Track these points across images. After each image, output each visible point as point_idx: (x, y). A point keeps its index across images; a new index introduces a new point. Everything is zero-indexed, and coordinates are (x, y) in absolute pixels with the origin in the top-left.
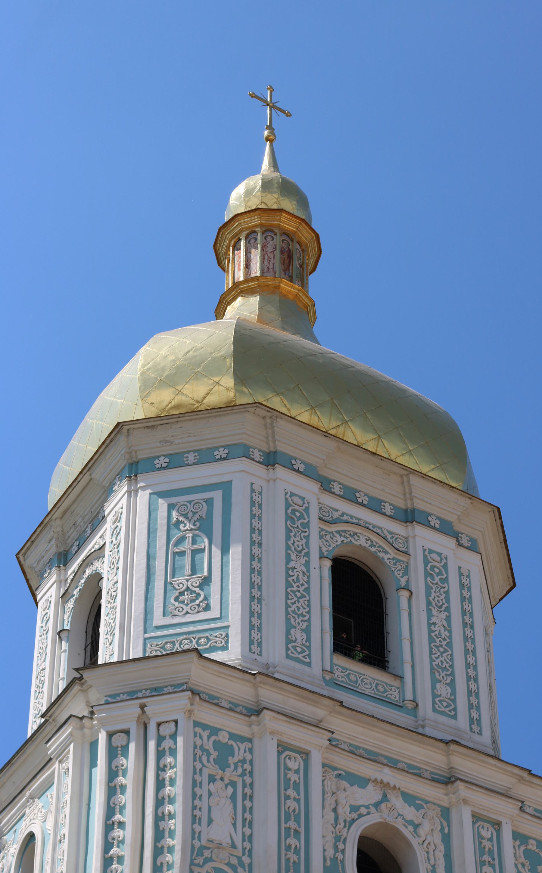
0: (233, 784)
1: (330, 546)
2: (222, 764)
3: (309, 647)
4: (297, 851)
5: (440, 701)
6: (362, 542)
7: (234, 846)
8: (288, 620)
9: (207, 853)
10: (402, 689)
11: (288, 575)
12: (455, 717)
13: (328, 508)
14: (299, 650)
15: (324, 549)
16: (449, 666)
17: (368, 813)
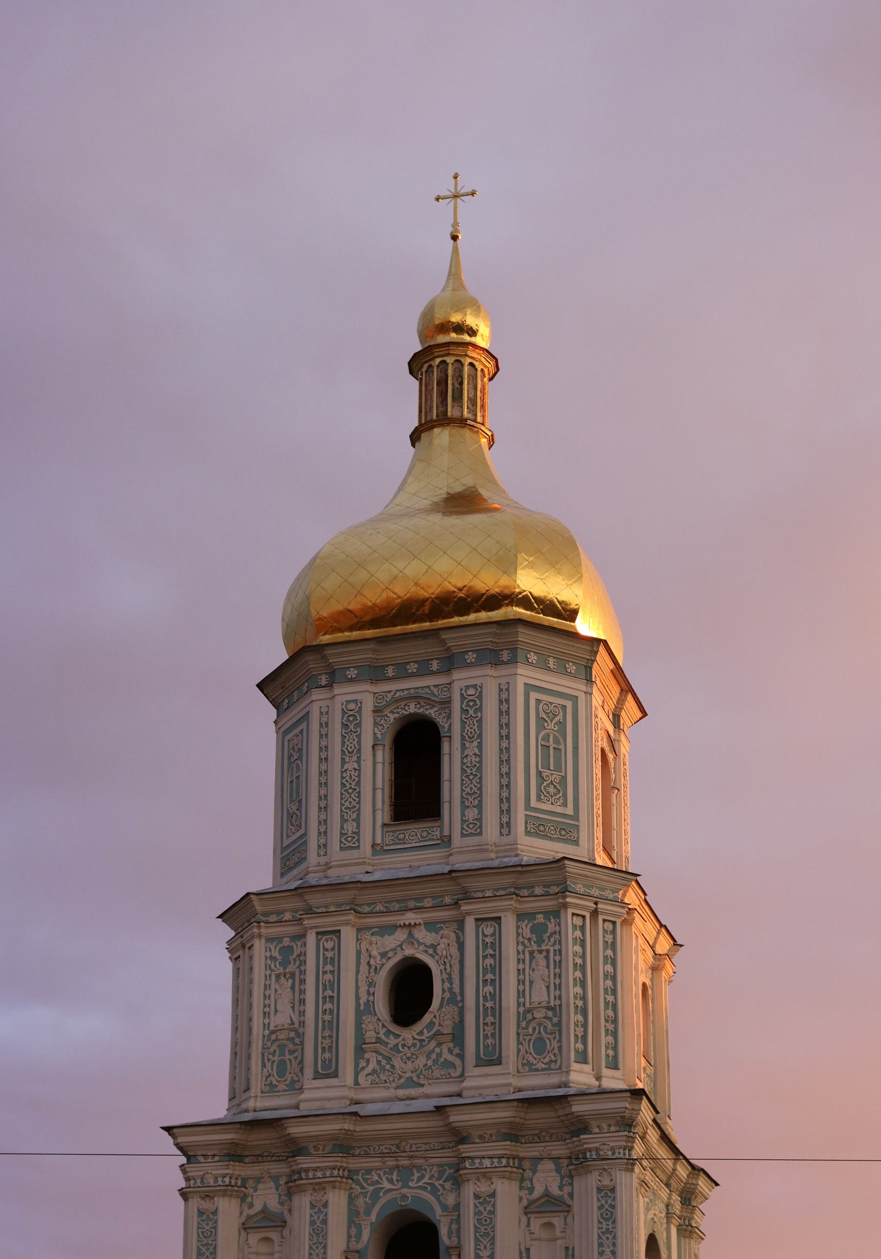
0: (293, 975)
1: (384, 728)
2: (285, 963)
3: (358, 833)
4: (331, 1012)
5: (467, 826)
6: (412, 709)
7: (293, 1023)
8: (342, 816)
9: (274, 1037)
10: (441, 827)
11: (342, 778)
12: (480, 834)
13: (383, 694)
14: (349, 839)
15: (379, 736)
16: (477, 790)
17: (395, 954)
